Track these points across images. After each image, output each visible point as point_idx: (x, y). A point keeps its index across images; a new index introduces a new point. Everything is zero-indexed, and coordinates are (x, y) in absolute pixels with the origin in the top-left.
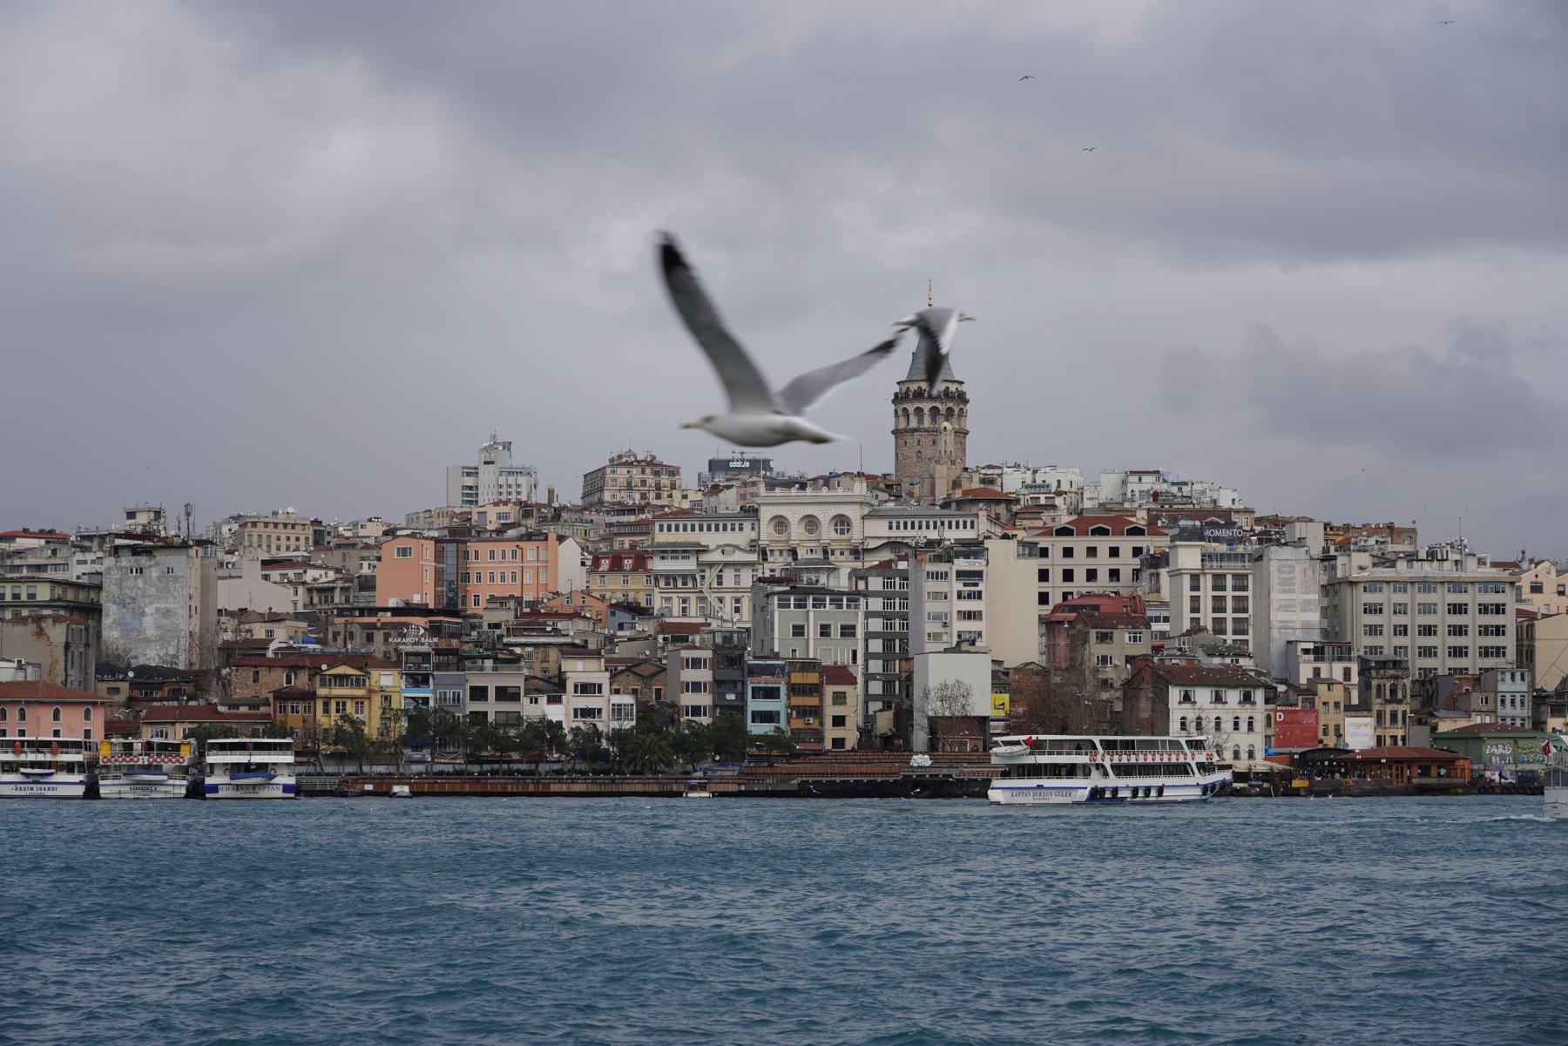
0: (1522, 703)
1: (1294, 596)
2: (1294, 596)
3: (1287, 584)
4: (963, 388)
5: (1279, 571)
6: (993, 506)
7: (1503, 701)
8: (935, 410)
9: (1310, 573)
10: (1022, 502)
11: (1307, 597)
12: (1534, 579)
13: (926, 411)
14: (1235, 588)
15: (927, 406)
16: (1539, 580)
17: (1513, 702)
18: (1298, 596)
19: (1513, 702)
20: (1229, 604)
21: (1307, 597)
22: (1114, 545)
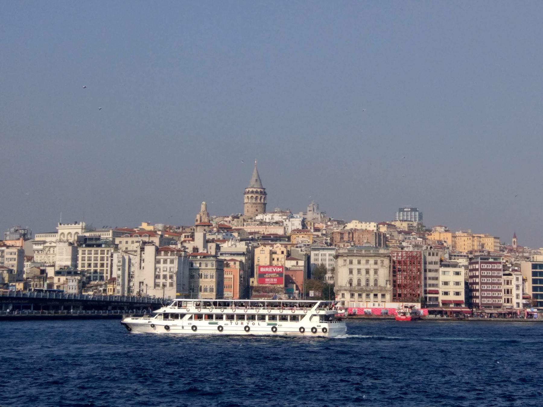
0: (75, 289)
1: (63, 257)
2: (63, 257)
3: (61, 253)
4: (266, 191)
5: (59, 250)
6: (203, 227)
7: (70, 288)
9: (68, 250)
10: (213, 226)
11: (67, 257)
13: (250, 197)
14: (95, 254)
17: (73, 288)
18: (65, 257)
19: (73, 288)
20: (86, 259)
21: (67, 257)
22: (127, 240)
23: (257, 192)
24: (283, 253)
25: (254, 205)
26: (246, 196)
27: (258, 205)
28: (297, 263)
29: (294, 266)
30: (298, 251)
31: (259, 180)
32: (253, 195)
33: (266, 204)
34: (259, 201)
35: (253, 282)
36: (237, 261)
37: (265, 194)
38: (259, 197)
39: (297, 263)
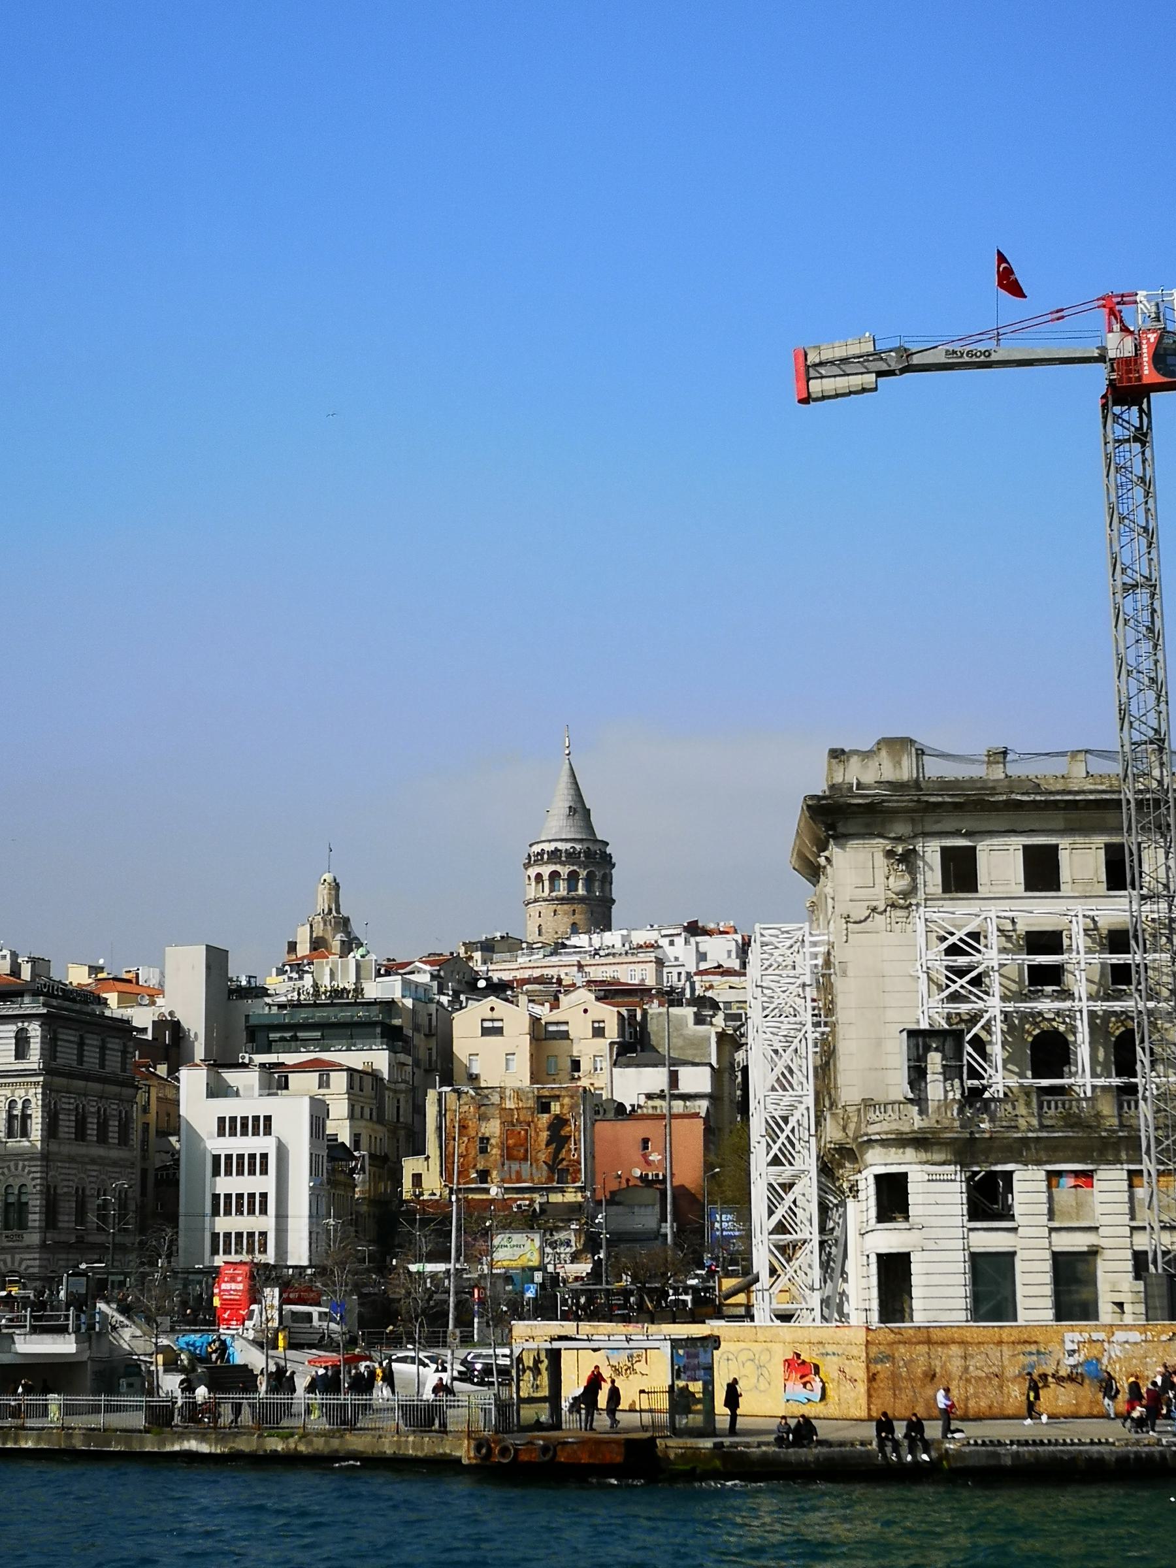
8: (554, 875)
12: (489, 1015)
13: (546, 877)
15: (546, 870)
16: (495, 1015)
23: (572, 857)
24: (599, 1032)
25: (566, 907)
26: (532, 872)
27: (579, 907)
28: (674, 1079)
29: (661, 1096)
30: (685, 1016)
31: (580, 811)
32: (558, 868)
33: (613, 901)
34: (581, 891)
35: (417, 1179)
36: (338, 1067)
37: (606, 861)
38: (583, 873)
39: (674, 1079)
